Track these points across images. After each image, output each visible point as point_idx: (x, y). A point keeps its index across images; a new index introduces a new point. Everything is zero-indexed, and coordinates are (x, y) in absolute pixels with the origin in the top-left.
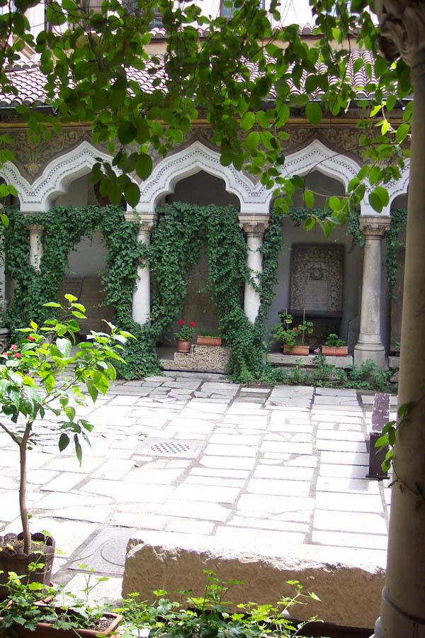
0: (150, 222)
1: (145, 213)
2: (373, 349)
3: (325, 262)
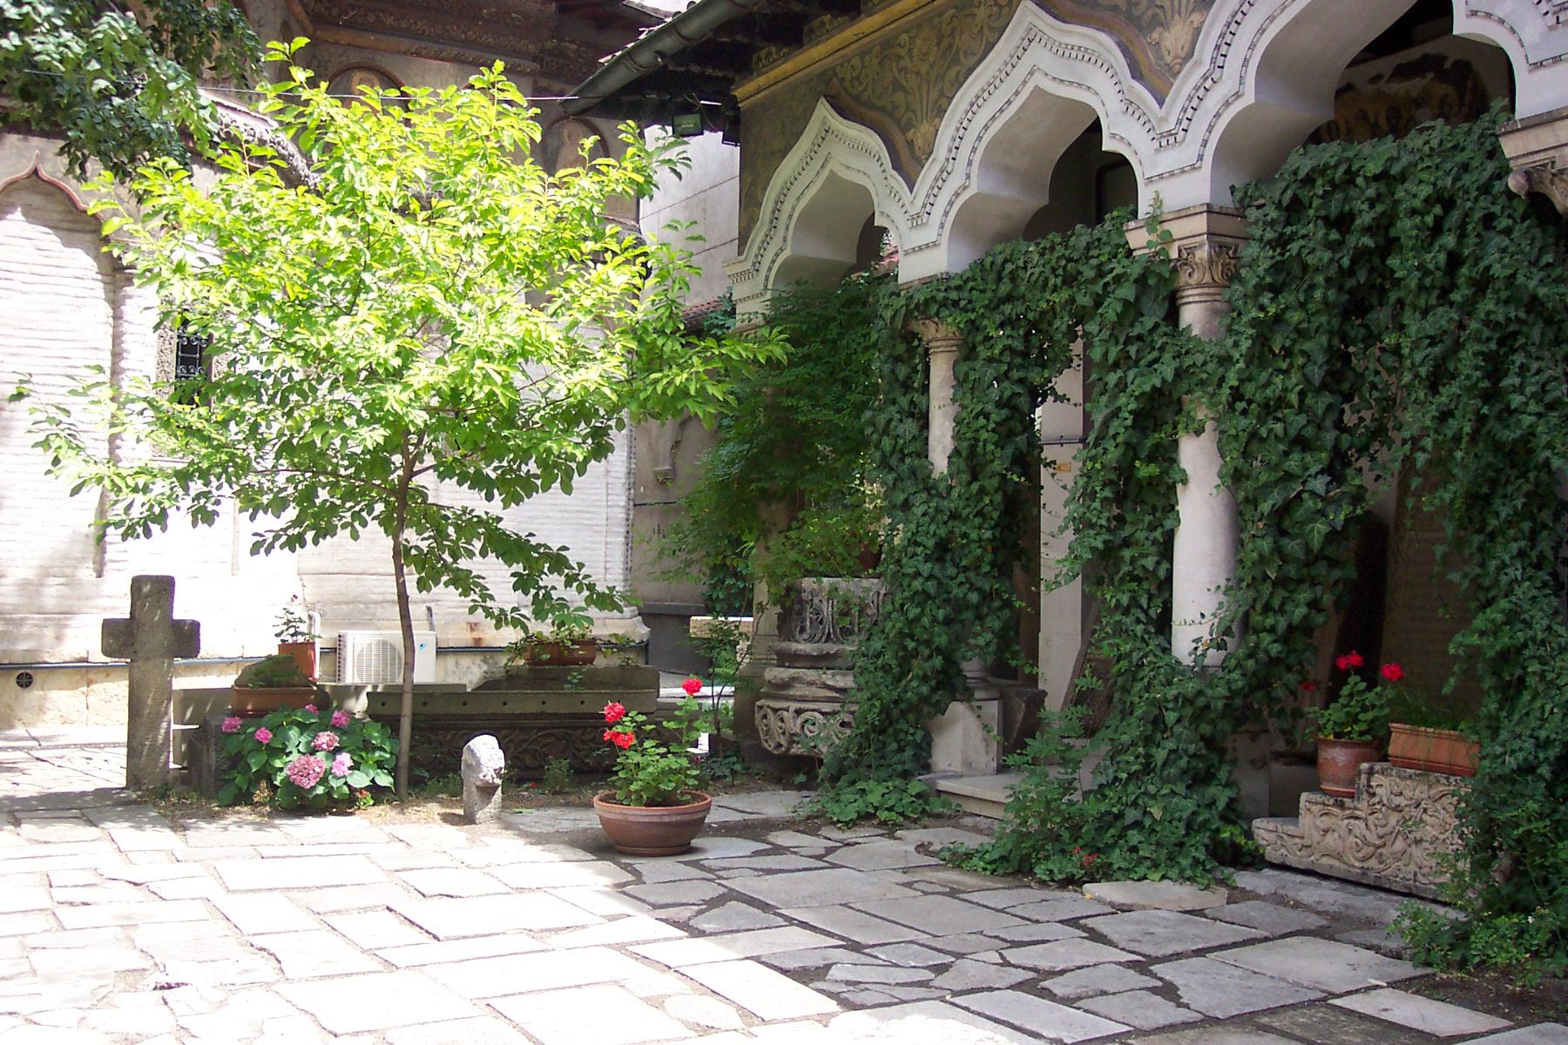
0: (1201, 246)
1: (1183, 214)
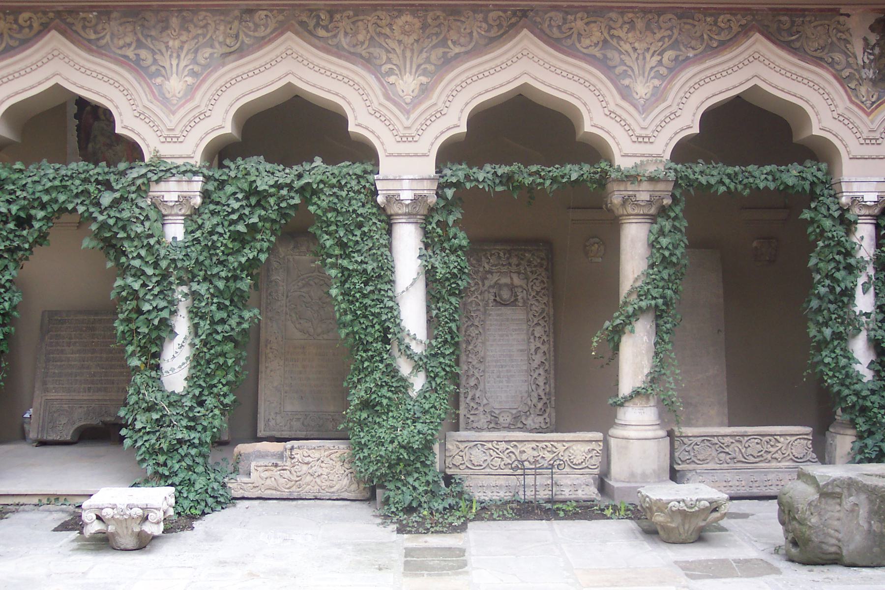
0: (195, 196)
2: (650, 434)
3: (519, 273)
